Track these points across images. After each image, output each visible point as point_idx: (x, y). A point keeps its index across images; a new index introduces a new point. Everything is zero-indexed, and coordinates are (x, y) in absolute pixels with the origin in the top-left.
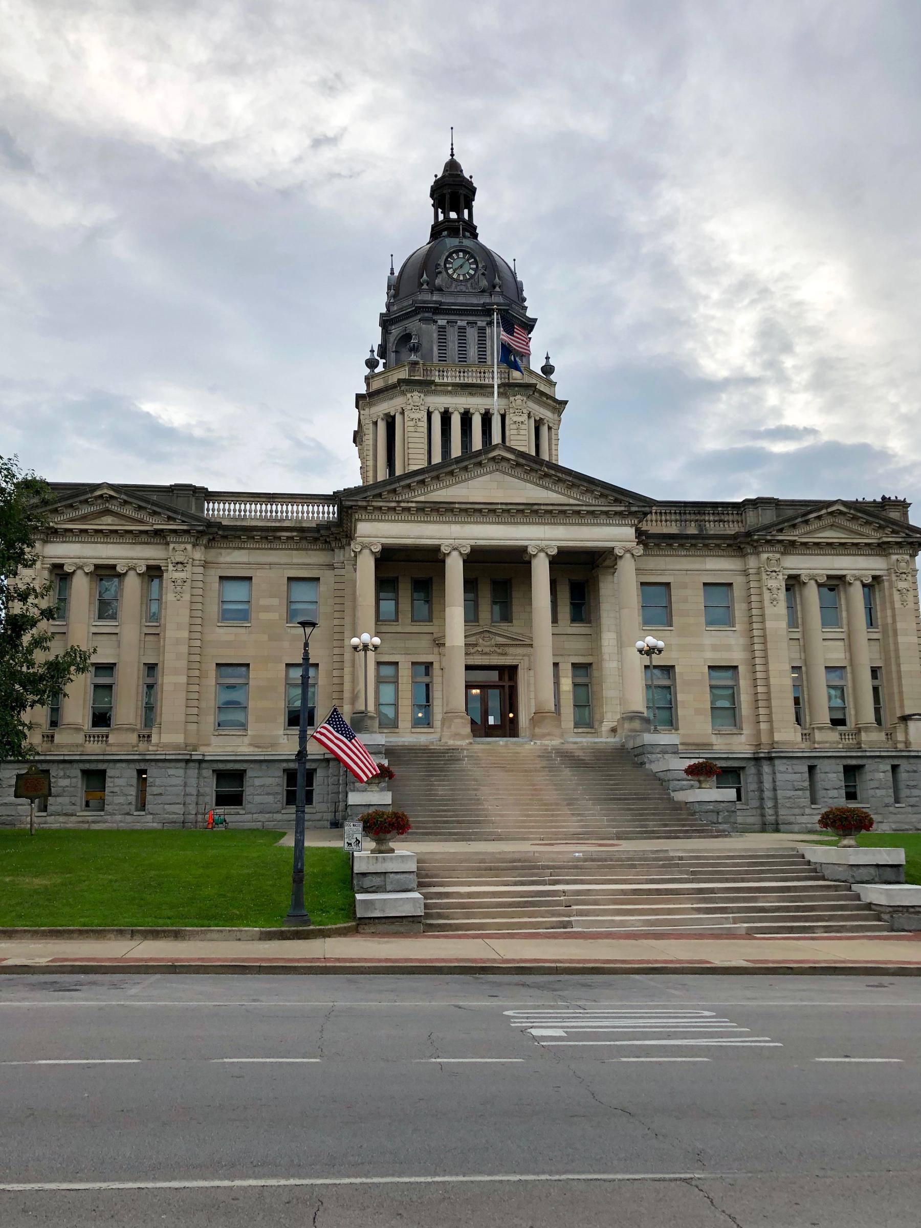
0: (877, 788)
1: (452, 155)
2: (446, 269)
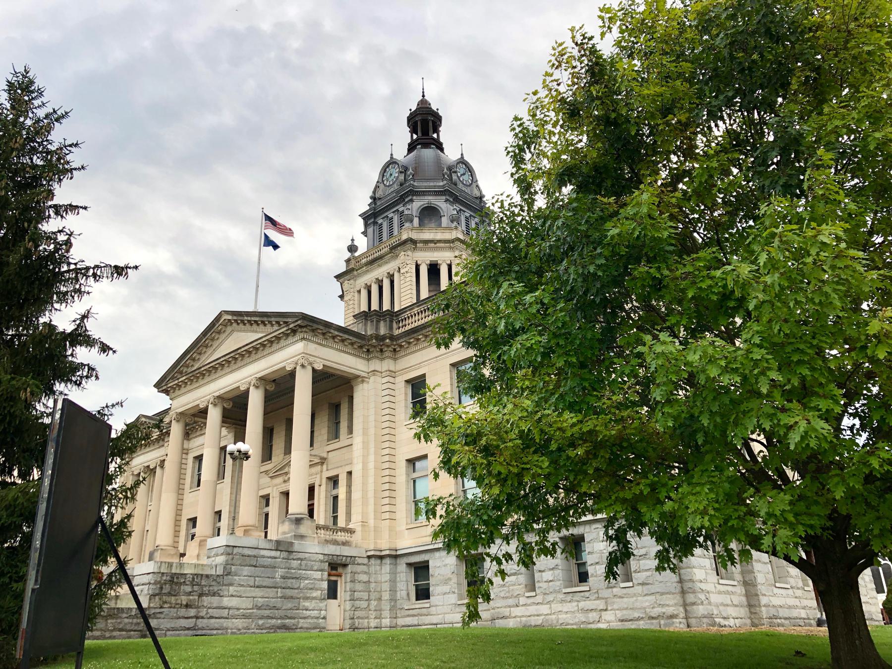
0: (597, 563)
1: (423, 96)
2: (383, 181)
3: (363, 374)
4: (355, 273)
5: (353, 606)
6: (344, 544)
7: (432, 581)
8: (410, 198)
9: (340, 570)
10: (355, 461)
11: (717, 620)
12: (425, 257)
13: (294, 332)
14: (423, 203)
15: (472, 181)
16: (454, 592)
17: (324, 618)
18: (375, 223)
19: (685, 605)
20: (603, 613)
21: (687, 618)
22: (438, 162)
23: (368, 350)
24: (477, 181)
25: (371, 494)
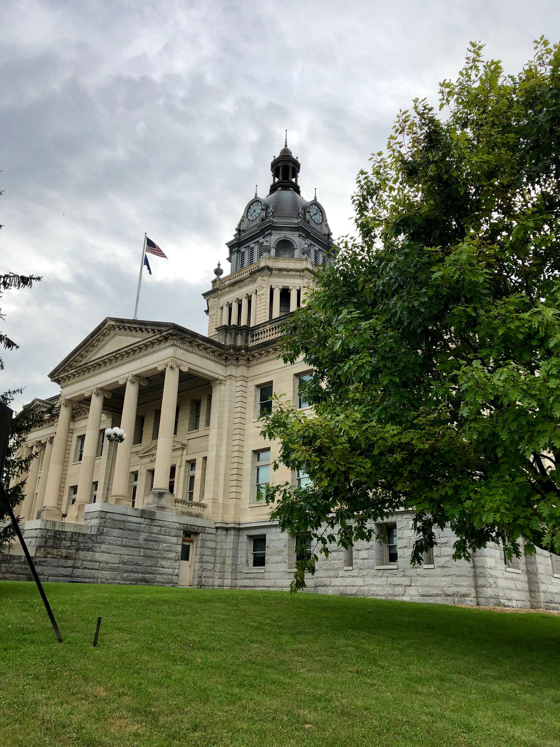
1: (286, 146)
2: (247, 216)
3: (221, 378)
4: (219, 292)
5: (202, 567)
6: (198, 516)
7: (267, 551)
8: (269, 231)
9: (193, 537)
10: (210, 449)
11: (502, 601)
12: (279, 283)
13: (166, 339)
14: (279, 237)
15: (322, 220)
16: (285, 562)
17: (177, 575)
18: (238, 251)
19: (476, 587)
20: (408, 588)
21: (477, 597)
22: (295, 203)
23: (226, 358)
24: (326, 221)
25: (222, 477)
